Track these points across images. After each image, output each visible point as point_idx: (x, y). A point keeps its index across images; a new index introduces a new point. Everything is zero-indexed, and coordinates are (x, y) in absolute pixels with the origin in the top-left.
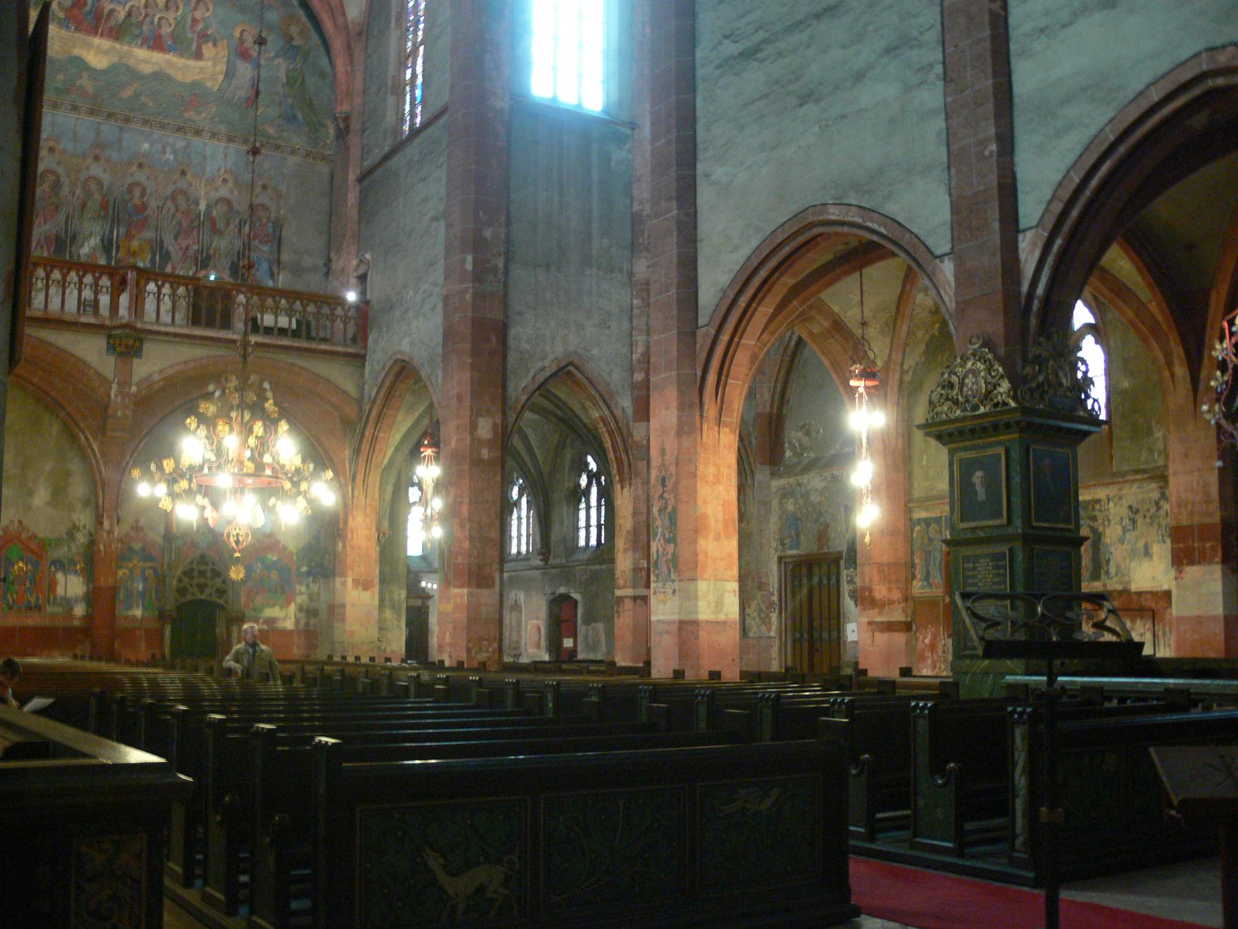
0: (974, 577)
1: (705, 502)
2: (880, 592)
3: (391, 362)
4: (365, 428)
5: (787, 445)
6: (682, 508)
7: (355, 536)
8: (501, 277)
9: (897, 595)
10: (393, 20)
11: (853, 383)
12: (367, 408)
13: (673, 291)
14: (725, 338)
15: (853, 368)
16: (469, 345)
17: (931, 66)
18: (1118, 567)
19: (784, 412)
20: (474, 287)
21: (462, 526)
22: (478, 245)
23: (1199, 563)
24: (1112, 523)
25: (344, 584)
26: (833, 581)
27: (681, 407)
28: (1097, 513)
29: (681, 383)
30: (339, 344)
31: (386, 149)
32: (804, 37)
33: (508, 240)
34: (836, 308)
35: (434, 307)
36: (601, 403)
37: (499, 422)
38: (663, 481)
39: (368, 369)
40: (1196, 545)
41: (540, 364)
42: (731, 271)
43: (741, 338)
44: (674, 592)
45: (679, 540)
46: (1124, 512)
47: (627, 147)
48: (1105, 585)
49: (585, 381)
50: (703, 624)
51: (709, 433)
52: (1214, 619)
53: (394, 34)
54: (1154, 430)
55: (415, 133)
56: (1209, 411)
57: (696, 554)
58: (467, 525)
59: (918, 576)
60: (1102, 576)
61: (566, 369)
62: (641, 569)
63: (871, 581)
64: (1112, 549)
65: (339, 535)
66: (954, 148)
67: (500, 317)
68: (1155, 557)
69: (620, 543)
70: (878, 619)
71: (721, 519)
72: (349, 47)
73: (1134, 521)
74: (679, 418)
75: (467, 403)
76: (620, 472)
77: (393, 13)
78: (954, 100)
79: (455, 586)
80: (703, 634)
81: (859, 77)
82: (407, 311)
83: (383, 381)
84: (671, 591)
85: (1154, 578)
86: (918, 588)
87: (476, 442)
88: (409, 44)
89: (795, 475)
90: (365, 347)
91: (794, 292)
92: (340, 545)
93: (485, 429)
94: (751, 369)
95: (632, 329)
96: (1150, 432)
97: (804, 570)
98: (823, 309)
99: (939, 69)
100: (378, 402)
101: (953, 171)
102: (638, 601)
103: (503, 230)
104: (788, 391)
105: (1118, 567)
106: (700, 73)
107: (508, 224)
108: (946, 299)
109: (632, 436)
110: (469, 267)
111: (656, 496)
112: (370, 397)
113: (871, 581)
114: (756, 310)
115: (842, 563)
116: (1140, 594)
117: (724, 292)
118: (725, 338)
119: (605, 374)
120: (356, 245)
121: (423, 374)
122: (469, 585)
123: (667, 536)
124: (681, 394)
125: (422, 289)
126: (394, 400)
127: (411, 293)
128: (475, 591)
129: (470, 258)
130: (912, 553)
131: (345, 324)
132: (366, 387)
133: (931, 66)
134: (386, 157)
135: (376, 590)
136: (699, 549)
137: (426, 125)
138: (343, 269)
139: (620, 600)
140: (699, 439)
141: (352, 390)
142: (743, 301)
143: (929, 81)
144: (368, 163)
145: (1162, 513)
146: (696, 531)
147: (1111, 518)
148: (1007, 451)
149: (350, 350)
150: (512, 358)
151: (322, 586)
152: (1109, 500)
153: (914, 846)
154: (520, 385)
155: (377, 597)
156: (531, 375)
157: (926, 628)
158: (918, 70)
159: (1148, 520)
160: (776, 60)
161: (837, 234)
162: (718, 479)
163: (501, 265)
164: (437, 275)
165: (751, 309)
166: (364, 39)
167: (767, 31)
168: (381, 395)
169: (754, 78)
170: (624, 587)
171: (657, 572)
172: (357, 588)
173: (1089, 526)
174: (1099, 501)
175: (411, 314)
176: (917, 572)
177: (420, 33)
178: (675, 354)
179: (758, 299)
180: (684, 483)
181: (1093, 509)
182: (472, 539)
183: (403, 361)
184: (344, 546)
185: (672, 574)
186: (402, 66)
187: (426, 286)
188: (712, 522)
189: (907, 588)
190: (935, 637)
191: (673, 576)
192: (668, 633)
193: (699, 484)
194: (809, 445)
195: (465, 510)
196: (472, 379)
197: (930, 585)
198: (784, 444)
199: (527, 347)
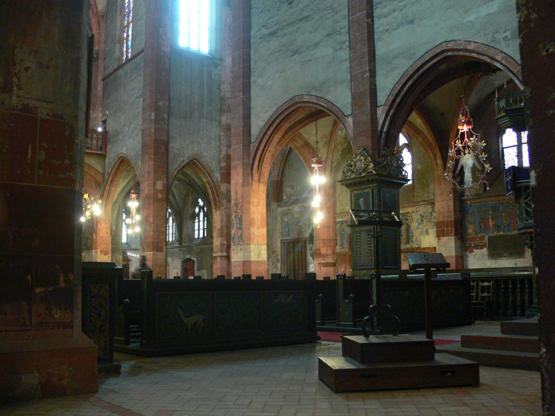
0: (360, 239)
1: (254, 213)
2: (323, 251)
3: (117, 158)
4: (106, 185)
5: (284, 194)
6: (244, 216)
7: (101, 232)
8: (166, 122)
9: (330, 252)
10: (119, 11)
11: (313, 165)
12: (106, 177)
13: (241, 129)
14: (262, 147)
15: (313, 159)
16: (153, 150)
17: (344, 42)
19: (283, 180)
20: (155, 127)
21: (150, 226)
22: (157, 108)
24: (414, 221)
25: (96, 252)
26: (304, 249)
27: (244, 175)
28: (408, 218)
29: (244, 165)
30: (94, 150)
31: (115, 67)
32: (295, 28)
33: (169, 107)
34: (306, 137)
35: (137, 135)
36: (207, 175)
37: (165, 182)
38: (236, 205)
39: (107, 161)
41: (182, 159)
42: (264, 120)
43: (268, 148)
44: (241, 249)
45: (243, 229)
46: (419, 217)
47: (218, 69)
48: (411, 246)
49: (201, 166)
50: (253, 262)
51: (255, 185)
52: (452, 257)
53: (119, 18)
54: (430, 185)
55: (128, 61)
56: (447, 175)
57: (250, 234)
58: (152, 225)
59: (339, 244)
60: (410, 242)
61: (193, 161)
62: (224, 245)
63: (319, 247)
64: (414, 232)
65: (94, 232)
66: (352, 74)
67: (166, 139)
68: (430, 234)
69: (215, 234)
70: (323, 262)
71: (260, 220)
72: (99, 22)
73: (422, 220)
74: (243, 179)
75: (152, 174)
76: (215, 205)
77: (119, 9)
78: (353, 56)
79: (147, 251)
80: (253, 266)
81: (317, 45)
82: (125, 136)
83: (114, 166)
84: (240, 249)
85: (430, 242)
86: (338, 249)
87: (156, 191)
88: (126, 22)
89: (288, 206)
90: (106, 151)
91: (290, 129)
92: (95, 236)
93: (160, 185)
94: (272, 160)
95: (220, 145)
96: (428, 186)
97: (291, 245)
98: (300, 136)
99: (348, 43)
100: (112, 175)
101: (352, 83)
102: (223, 258)
103: (167, 103)
104: (285, 172)
105: (416, 238)
106: (252, 41)
107: (169, 100)
108: (349, 132)
109: (220, 189)
110: (153, 117)
111: (234, 211)
112: (108, 172)
113: (319, 247)
114: (274, 136)
115: (307, 242)
116: (424, 248)
117: (262, 129)
118: (262, 147)
119: (209, 164)
120: (102, 108)
121: (132, 163)
122: (153, 251)
123: (238, 227)
124: (244, 169)
125: (132, 127)
126: (118, 174)
127: (127, 128)
128: (155, 253)
129: (153, 114)
130: (336, 235)
131: (97, 141)
132: (106, 168)
133: (344, 42)
134: (116, 70)
135: (110, 255)
136: (251, 233)
137: (133, 57)
138: (95, 118)
139: (216, 257)
140: (251, 188)
141: (100, 169)
142: (269, 133)
143: (344, 48)
144: (107, 72)
145: (433, 217)
146: (250, 225)
147: (413, 219)
148: (372, 190)
149: (99, 152)
150: (171, 156)
151: (86, 255)
152: (413, 212)
153: (338, 325)
154: (174, 168)
155: (110, 258)
156: (179, 163)
157: (342, 265)
158: (339, 44)
159: (427, 220)
160: (283, 37)
161: (307, 106)
162: (258, 205)
163: (166, 116)
164: (139, 120)
165: (273, 136)
166: (105, 18)
167: (280, 25)
168: (113, 172)
169: (274, 44)
170: (217, 252)
171: (234, 242)
172: (102, 254)
174: (409, 213)
175: (127, 137)
176: (338, 243)
177: (131, 18)
178: (241, 154)
179: (275, 131)
180: (245, 206)
181: (407, 216)
182: (154, 231)
183: (123, 157)
184: (96, 236)
185: (240, 242)
186: (122, 31)
187: (134, 125)
188: (256, 221)
189: (334, 249)
190: (345, 269)
191: (241, 243)
192: (239, 266)
193: (251, 206)
194: (293, 193)
195: (151, 219)
196: (154, 164)
197: (343, 248)
198: (282, 193)
199: (177, 151)
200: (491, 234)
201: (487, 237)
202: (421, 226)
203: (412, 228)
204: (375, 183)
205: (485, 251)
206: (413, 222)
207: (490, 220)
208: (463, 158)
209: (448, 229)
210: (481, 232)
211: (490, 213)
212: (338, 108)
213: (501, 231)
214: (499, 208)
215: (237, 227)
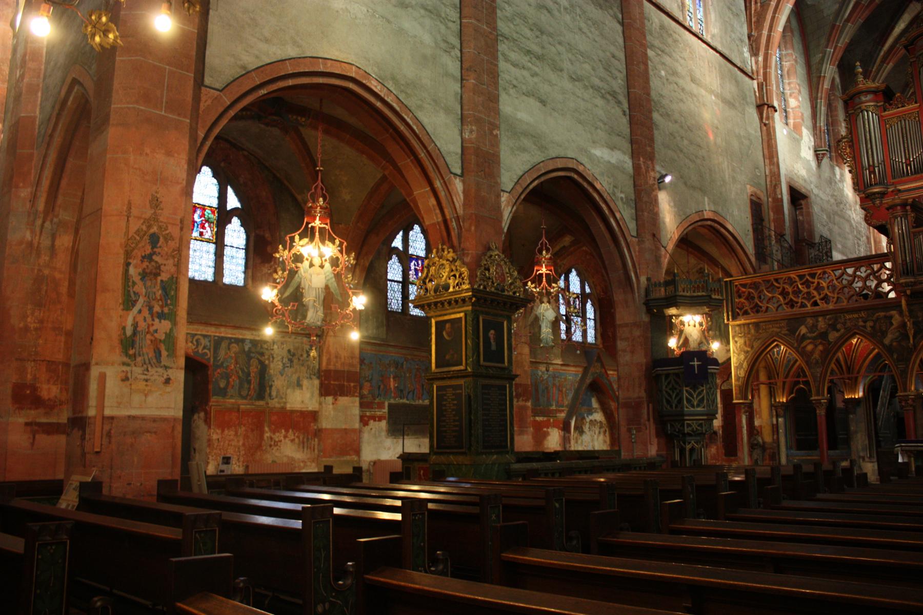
18: (278, 391)
23: (347, 396)
24: (275, 360)
28: (264, 351)
40: (346, 383)
46: (285, 353)
48: (267, 403)
64: (275, 379)
68: (304, 387)
73: (291, 361)
85: (303, 402)
105: (278, 391)
113: (35, 378)
116: (292, 412)
147: (275, 356)
148: (466, 315)
159: (301, 362)
173: (258, 359)
200: (392, 401)
201: (386, 404)
202: (289, 371)
203: (272, 371)
204: (467, 306)
205: (384, 424)
206: (273, 362)
207: (392, 380)
208: (538, 308)
209: (350, 385)
210: (379, 395)
211: (392, 370)
212: (439, 150)
213: (404, 398)
214: (402, 364)
215: (151, 308)
